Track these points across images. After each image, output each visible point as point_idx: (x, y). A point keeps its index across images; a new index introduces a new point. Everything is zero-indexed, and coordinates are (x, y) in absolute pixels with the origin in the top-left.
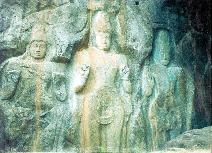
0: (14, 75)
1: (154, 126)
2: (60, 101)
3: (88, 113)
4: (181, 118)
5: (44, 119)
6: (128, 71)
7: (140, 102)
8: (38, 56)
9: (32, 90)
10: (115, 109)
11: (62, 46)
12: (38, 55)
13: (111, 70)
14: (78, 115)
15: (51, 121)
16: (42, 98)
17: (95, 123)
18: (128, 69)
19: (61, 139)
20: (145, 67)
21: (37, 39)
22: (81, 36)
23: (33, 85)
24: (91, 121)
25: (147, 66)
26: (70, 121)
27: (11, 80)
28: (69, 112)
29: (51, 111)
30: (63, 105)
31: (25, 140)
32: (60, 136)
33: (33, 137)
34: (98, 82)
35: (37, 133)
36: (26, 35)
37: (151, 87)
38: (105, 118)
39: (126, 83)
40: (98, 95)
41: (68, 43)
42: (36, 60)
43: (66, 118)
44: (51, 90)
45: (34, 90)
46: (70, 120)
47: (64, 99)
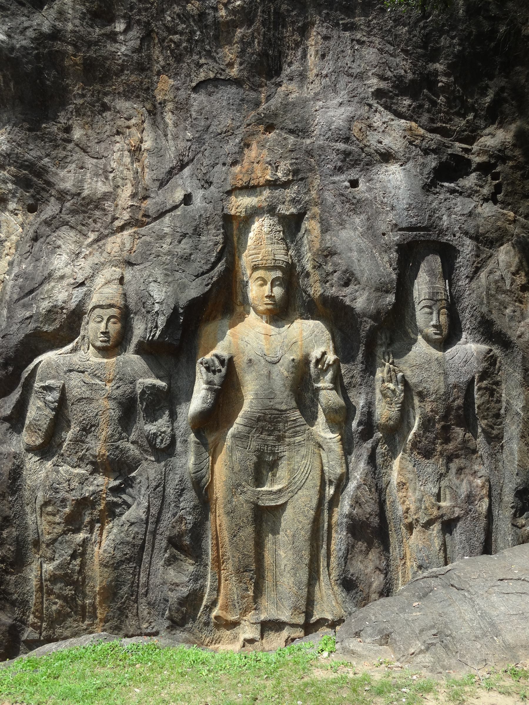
1: (408, 509)
3: (224, 479)
10: (296, 467)
17: (243, 504)
19: (162, 542)
22: (207, 285)
23: (91, 414)
26: (181, 500)
28: (178, 476)
31: (73, 546)
35: (102, 529)
38: (270, 489)
45: (94, 426)
46: (181, 495)
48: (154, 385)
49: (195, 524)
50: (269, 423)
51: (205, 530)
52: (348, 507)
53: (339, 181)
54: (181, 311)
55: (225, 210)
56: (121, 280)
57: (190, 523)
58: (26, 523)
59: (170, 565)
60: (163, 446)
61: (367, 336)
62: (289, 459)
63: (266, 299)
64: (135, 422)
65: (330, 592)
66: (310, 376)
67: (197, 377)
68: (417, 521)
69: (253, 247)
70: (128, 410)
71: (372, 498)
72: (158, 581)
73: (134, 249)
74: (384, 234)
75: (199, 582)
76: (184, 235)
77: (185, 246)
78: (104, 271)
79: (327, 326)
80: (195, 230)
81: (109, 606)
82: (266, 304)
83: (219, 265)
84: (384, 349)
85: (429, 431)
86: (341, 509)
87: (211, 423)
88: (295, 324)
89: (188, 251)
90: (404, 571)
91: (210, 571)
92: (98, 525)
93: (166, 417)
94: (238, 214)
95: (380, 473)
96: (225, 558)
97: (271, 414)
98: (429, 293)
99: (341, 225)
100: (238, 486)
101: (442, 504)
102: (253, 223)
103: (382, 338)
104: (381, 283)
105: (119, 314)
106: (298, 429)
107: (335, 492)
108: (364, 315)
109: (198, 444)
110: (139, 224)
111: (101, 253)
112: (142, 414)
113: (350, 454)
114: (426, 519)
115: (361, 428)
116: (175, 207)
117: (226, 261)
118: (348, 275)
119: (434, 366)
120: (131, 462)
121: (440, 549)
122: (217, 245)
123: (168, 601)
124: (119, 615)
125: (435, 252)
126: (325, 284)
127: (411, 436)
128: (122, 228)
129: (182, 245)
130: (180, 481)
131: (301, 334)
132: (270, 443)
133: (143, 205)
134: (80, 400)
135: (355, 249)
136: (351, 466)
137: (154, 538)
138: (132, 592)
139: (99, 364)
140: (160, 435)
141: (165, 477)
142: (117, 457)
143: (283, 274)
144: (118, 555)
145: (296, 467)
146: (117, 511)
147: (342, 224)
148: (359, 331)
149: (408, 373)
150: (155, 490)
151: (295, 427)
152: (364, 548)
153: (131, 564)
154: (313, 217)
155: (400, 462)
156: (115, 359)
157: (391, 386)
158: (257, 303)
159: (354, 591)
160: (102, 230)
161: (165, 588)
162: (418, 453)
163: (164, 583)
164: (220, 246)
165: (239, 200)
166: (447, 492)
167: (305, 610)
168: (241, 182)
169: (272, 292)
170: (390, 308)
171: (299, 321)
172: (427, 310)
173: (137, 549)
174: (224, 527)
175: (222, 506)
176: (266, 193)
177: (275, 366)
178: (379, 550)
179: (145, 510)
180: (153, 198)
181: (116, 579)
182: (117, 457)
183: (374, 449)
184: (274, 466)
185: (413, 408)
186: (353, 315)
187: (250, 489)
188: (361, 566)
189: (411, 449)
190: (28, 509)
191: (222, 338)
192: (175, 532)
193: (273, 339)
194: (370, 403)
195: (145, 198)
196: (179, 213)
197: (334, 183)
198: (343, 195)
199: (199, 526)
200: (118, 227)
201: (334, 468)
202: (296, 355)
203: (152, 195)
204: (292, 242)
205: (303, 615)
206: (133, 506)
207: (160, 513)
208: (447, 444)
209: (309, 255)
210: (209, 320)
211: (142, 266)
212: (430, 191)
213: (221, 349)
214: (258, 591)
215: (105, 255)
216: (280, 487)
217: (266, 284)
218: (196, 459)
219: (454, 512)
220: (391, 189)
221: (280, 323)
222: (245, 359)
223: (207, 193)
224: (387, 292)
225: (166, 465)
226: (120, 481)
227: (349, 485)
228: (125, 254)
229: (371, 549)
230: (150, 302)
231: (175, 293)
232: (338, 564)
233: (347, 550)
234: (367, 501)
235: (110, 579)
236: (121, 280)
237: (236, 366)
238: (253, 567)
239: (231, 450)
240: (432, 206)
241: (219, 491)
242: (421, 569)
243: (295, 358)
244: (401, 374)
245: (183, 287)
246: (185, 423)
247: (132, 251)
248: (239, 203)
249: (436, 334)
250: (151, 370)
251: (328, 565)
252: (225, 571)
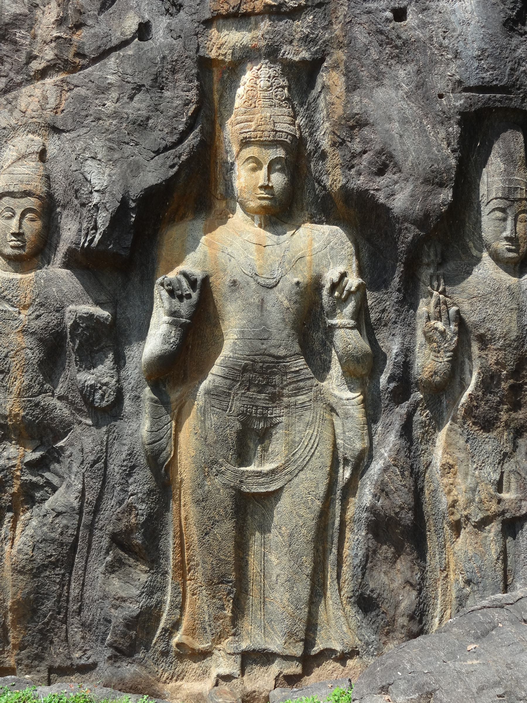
1: (455, 501)
3: (193, 454)
10: (297, 439)
16: (29, 401)
17: (219, 490)
22: (172, 167)
24: (204, 480)
26: (130, 481)
28: (126, 448)
35: (15, 520)
38: (259, 469)
39: (347, 337)
43: (116, 469)
46: (130, 475)
48: (91, 315)
49: (149, 515)
50: (259, 374)
51: (164, 525)
52: (370, 497)
53: (377, 9)
54: (133, 205)
55: (201, 50)
56: (42, 155)
57: (142, 515)
59: (113, 572)
60: (104, 404)
61: (409, 251)
62: (288, 426)
63: (259, 191)
64: (64, 369)
65: (340, 613)
66: (322, 308)
67: (155, 305)
68: (467, 518)
69: (243, 110)
70: (54, 349)
71: (404, 486)
72: (96, 594)
73: (62, 107)
74: (441, 96)
75: (155, 596)
76: (138, 88)
77: (140, 105)
78: (16, 140)
79: (349, 234)
80: (155, 80)
81: (26, 628)
82: (260, 198)
83: (191, 136)
84: (431, 271)
85: (491, 393)
86: (360, 500)
87: (175, 371)
88: (301, 230)
89: (144, 113)
90: (445, 586)
91: (170, 581)
92: (10, 514)
93: (109, 362)
94: (221, 58)
95: (417, 449)
96: (192, 563)
97: (264, 362)
98: (504, 188)
99: (377, 79)
100: (213, 464)
101: (505, 495)
102: (244, 72)
103: (430, 255)
104: (433, 172)
105: (40, 206)
106: (301, 384)
107: (352, 475)
108: (406, 219)
109: (156, 402)
110: (69, 68)
111: (11, 111)
112: (73, 356)
113: (375, 421)
114: (481, 516)
115: (392, 385)
116: (125, 43)
117: (202, 131)
118: (383, 158)
119: (505, 299)
120: (57, 426)
121: (498, 559)
122: (187, 104)
123: (110, 622)
124: (41, 639)
125: (515, 126)
126: (350, 169)
127: (464, 399)
128: (43, 74)
129: (135, 104)
131: (311, 245)
132: (261, 404)
133: (75, 37)
135: (396, 118)
136: (376, 438)
137: (91, 535)
138: (59, 608)
139: (10, 281)
140: (100, 388)
141: (107, 449)
142: (37, 418)
143: (287, 153)
144: (39, 557)
145: (297, 439)
146: (38, 495)
147: (378, 78)
148: (396, 243)
149: (466, 307)
150: (92, 466)
151: (298, 381)
152: (390, 555)
153: (58, 571)
154: (335, 67)
155: (447, 435)
156: (33, 274)
157: (440, 325)
158: (245, 196)
159: (374, 613)
160: (12, 75)
161: (107, 604)
162: (474, 423)
163: (105, 597)
164: (192, 108)
165: (222, 35)
166: (513, 480)
167: (303, 637)
168: (226, 7)
169: (269, 180)
170: (444, 209)
171: (308, 225)
172: (499, 214)
173: (66, 550)
174: (192, 521)
175: (190, 491)
176: (265, 25)
177: (271, 291)
178: (411, 557)
179: (77, 494)
180: (91, 27)
181: (37, 590)
182: (37, 418)
183: (410, 415)
184: (265, 436)
185: (470, 358)
186: (389, 219)
187: (230, 469)
188: (385, 579)
189: (464, 418)
191: (193, 248)
192: (122, 526)
193: (269, 252)
194: (408, 349)
195: (78, 26)
196: (130, 52)
197: (369, 12)
198: (381, 32)
199: (156, 519)
200: (37, 72)
201: (352, 442)
202: (302, 276)
203: (90, 22)
204: (302, 104)
205: (301, 644)
206: (61, 489)
207: (100, 499)
208: (516, 411)
209: (327, 124)
210: (174, 221)
211: (73, 134)
212: (514, 30)
213: (191, 264)
214: (239, 610)
215: (17, 114)
216: (273, 466)
218: (152, 425)
219: (520, 507)
220: (456, 25)
221: (280, 229)
222: (227, 280)
223: (175, 21)
224: (442, 185)
225: (108, 432)
226: (41, 453)
227: (372, 465)
228: (48, 114)
229: (399, 556)
230: (85, 190)
231: (124, 178)
232: (353, 576)
233: (367, 557)
234: (397, 490)
235: (26, 591)
236: (42, 155)
237: (213, 289)
238: (232, 578)
239: (204, 412)
240: (517, 54)
241: (186, 469)
242: (469, 585)
243: (301, 280)
244: (455, 308)
245: (136, 169)
246: (137, 371)
247: (59, 110)
248: (224, 41)
249: (509, 250)
250: (88, 293)
251: (339, 577)
252: (192, 582)
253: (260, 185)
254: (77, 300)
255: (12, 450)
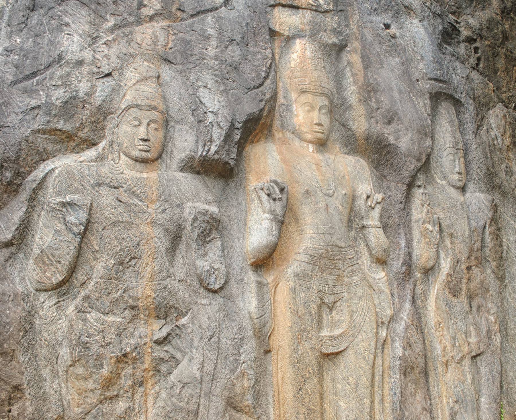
0: (73, 209)
1: (445, 347)
2: (209, 290)
3: (290, 325)
4: (498, 322)
5: (165, 348)
6: (379, 200)
7: (409, 286)
8: (143, 153)
9: (127, 260)
10: (355, 310)
11: (213, 125)
12: (145, 151)
13: (340, 198)
14: (261, 331)
15: (184, 353)
16: (159, 284)
17: (308, 352)
18: (379, 197)
20: (418, 193)
21: (139, 102)
23: (131, 244)
25: (421, 191)
27: (64, 227)
29: (183, 321)
30: (219, 301)
32: (214, 398)
33: (137, 406)
34: (309, 232)
35: (146, 394)
36: (108, 90)
37: (434, 245)
38: (332, 334)
40: (312, 272)
41: (229, 118)
42: (138, 166)
43: (229, 342)
44: (183, 257)
46: (241, 346)
47: (220, 286)
58: (44, 393)
92: (141, 389)
101: (471, 340)
114: (460, 355)
130: (240, 328)
134: (115, 224)
141: (219, 325)
150: (209, 340)
179: (199, 366)
182: (165, 299)
190: (46, 372)
216: (340, 331)
217: (314, 110)
218: (259, 302)
253: (315, 122)
254: (195, 197)
255: (142, 329)
